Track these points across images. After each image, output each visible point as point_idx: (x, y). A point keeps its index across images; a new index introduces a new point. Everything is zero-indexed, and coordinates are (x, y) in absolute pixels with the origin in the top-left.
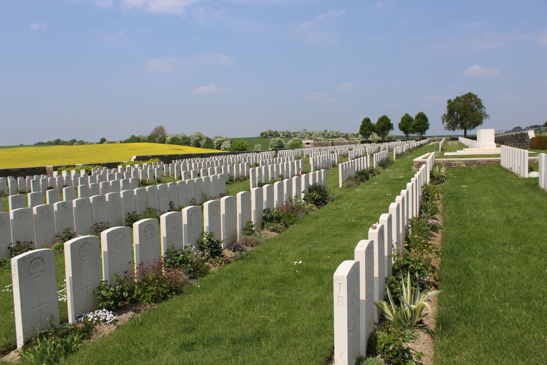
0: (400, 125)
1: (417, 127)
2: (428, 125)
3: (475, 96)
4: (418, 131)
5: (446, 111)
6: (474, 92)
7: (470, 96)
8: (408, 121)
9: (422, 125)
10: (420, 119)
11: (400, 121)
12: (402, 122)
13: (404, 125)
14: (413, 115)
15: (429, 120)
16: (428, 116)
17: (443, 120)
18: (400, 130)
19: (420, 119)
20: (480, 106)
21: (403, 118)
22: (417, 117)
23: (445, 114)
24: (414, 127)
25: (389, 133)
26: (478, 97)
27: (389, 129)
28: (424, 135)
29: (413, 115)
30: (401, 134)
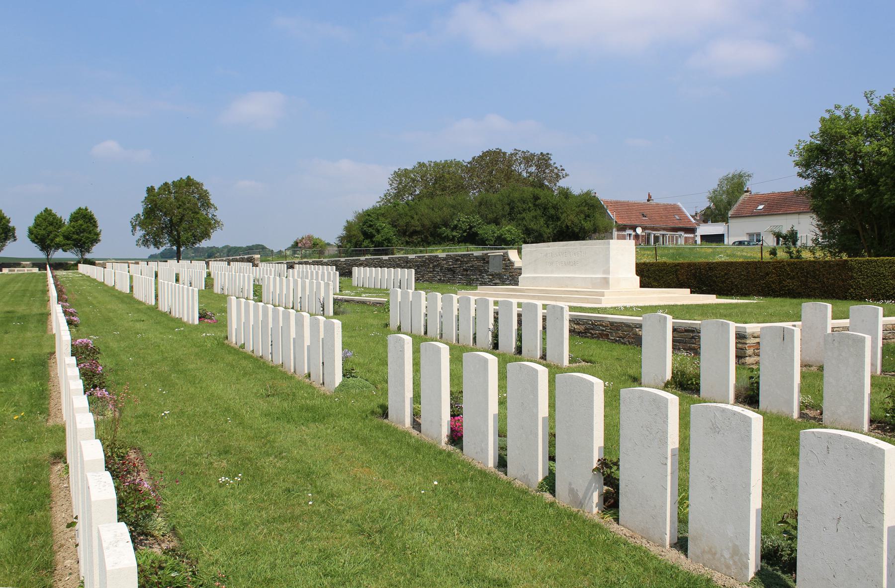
0: (31, 232)
1: (75, 236)
2: (98, 234)
3: (198, 185)
4: (76, 245)
5: (140, 211)
6: (197, 178)
7: (189, 182)
8: (51, 224)
9: (86, 234)
10: (80, 222)
11: (31, 223)
12: (37, 225)
13: (44, 232)
14: (64, 214)
15: (99, 223)
16: (97, 217)
17: (134, 227)
18: (33, 241)
19: (80, 222)
20: (207, 204)
21: (38, 217)
22: (74, 218)
23: (138, 215)
24: (67, 238)
25: (5, 248)
26: (205, 188)
27: (6, 239)
28: (88, 256)
29: (64, 214)
30: (36, 253)
